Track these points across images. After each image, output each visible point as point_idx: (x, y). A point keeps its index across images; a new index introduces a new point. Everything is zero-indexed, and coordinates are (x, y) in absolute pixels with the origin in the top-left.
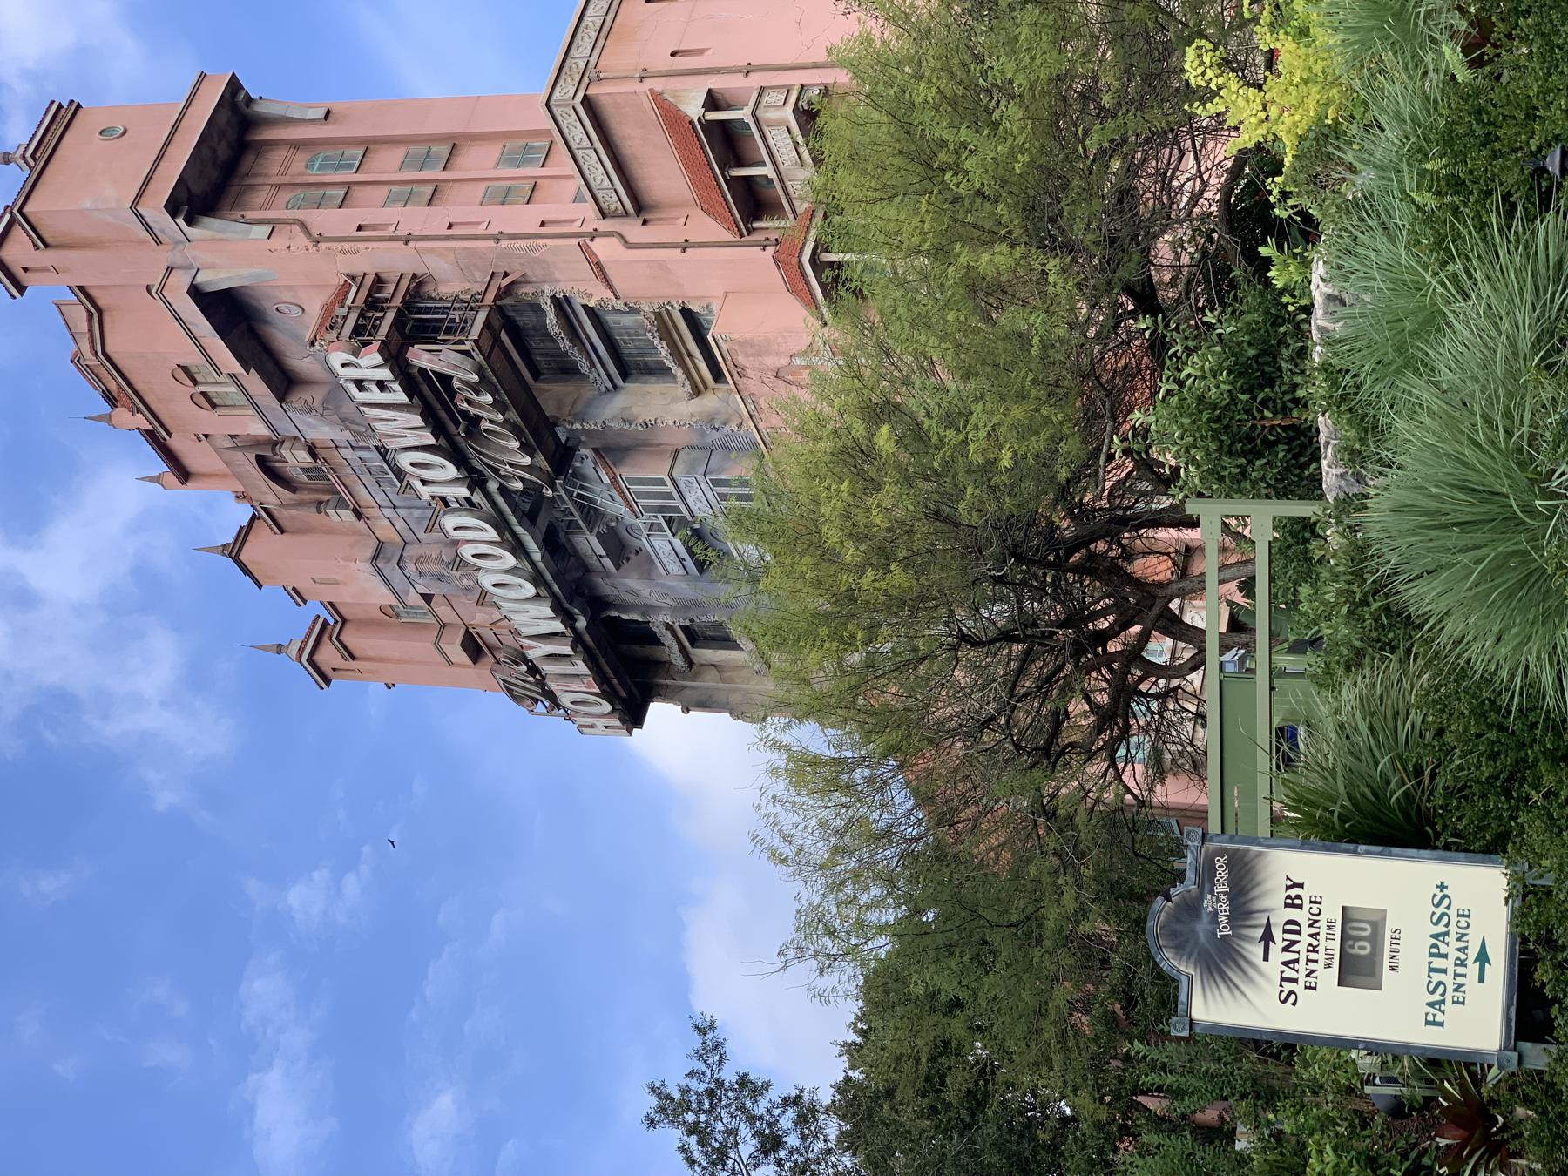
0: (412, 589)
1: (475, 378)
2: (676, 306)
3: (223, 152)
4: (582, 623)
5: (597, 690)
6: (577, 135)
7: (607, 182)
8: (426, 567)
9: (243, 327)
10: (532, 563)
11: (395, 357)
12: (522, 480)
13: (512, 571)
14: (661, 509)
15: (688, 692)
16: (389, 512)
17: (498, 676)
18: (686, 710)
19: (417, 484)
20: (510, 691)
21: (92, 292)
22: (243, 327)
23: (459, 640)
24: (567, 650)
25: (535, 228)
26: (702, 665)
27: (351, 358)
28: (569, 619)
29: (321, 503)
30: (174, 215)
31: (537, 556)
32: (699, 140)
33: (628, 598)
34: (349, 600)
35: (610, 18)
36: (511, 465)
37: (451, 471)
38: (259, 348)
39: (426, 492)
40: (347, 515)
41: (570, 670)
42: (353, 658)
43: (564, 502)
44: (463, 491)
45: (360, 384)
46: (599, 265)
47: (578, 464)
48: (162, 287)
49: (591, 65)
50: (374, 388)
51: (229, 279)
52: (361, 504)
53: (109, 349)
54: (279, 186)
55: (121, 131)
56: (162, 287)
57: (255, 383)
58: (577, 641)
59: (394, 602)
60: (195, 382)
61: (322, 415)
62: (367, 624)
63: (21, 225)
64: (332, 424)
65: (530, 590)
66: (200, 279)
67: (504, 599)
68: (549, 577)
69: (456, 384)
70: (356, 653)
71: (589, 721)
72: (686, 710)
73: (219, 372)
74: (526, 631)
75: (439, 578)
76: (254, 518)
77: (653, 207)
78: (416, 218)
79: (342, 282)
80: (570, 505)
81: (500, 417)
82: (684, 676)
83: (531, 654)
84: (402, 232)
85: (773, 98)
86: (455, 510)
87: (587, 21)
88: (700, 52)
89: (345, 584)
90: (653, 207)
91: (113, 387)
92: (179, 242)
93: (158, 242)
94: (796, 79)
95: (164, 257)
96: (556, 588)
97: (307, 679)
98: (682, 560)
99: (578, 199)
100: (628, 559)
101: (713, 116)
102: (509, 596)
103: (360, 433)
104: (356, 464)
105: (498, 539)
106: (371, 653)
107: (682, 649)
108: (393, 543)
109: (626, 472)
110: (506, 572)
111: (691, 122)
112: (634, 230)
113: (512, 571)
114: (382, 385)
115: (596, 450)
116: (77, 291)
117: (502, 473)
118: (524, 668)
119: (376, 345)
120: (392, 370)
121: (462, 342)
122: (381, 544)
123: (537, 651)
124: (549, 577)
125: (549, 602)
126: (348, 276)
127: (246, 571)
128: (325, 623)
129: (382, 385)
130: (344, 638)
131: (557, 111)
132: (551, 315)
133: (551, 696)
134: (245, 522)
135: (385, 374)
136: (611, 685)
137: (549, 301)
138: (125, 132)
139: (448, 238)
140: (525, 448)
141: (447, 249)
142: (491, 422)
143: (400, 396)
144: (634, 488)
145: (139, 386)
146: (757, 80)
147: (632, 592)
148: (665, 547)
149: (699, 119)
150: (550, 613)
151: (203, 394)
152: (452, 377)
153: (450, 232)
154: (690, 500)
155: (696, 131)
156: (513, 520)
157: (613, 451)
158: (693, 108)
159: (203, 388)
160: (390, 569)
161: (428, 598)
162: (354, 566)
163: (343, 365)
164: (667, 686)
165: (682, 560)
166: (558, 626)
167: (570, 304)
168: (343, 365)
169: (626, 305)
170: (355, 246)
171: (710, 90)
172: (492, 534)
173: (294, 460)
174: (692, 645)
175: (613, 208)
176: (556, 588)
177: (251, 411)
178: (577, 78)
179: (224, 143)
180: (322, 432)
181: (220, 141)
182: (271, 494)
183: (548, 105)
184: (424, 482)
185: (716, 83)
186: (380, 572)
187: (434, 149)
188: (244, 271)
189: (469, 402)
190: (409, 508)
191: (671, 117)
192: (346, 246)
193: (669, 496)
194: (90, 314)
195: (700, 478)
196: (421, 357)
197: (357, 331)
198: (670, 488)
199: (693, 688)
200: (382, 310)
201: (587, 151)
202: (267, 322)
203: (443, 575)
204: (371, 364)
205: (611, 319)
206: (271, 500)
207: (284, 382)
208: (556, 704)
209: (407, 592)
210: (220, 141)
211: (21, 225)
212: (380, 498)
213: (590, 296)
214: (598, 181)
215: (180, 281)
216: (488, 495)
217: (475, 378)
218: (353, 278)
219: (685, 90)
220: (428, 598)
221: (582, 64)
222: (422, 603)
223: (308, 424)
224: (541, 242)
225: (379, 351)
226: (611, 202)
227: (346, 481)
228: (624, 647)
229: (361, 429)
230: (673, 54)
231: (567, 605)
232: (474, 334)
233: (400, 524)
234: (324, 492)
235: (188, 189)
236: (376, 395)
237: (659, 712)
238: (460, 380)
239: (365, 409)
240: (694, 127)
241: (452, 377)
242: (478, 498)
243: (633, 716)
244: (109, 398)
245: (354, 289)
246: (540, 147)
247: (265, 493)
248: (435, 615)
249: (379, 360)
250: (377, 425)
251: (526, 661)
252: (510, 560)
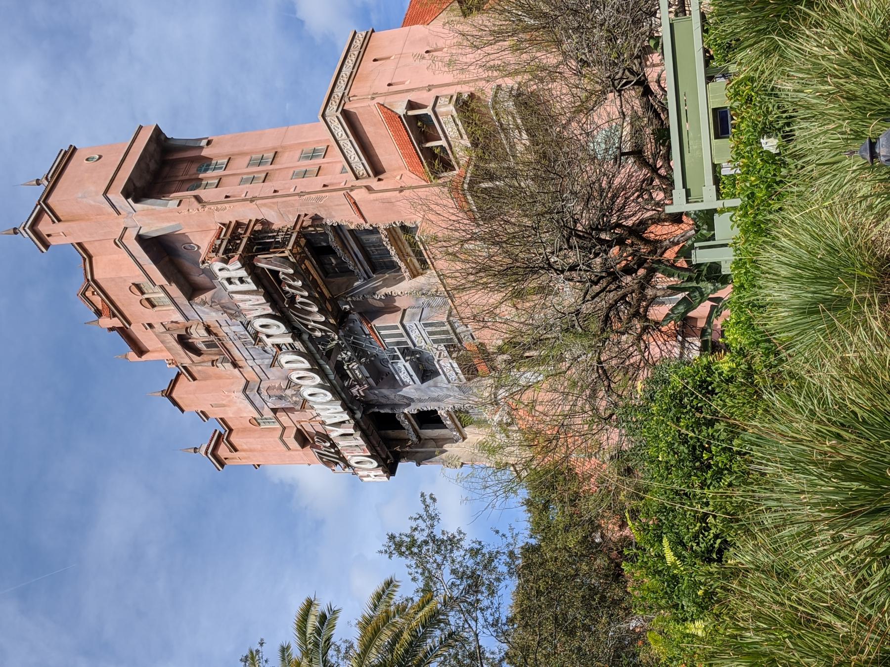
0: (265, 406)
1: (291, 271)
2: (398, 224)
3: (153, 166)
4: (358, 415)
5: (369, 454)
6: (339, 132)
7: (357, 158)
8: (271, 393)
9: (167, 259)
10: (330, 381)
11: (248, 263)
12: (321, 330)
14: (398, 343)
15: (419, 455)
16: (251, 362)
17: (314, 450)
18: (419, 464)
19: (264, 338)
20: (321, 459)
21: (87, 246)
22: (167, 259)
23: (293, 436)
24: (352, 431)
25: (320, 188)
26: (426, 439)
27: (224, 265)
28: (352, 413)
29: (213, 361)
30: (127, 197)
31: (332, 377)
32: (406, 129)
33: (383, 401)
34: (231, 416)
35: (355, 70)
36: (315, 322)
37: (283, 328)
38: (176, 271)
39: (269, 341)
40: (228, 366)
41: (354, 443)
42: (236, 450)
45: (229, 280)
46: (355, 203)
47: (352, 325)
48: (121, 238)
49: (346, 94)
50: (238, 282)
51: (157, 230)
52: (236, 359)
53: (96, 277)
54: (183, 181)
55: (98, 157)
56: (121, 238)
57: (174, 290)
58: (357, 426)
59: (257, 416)
60: (143, 293)
61: (211, 306)
62: (244, 430)
63: (47, 214)
64: (218, 310)
65: (330, 396)
66: (141, 232)
67: (315, 402)
68: (339, 389)
69: (282, 276)
70: (238, 448)
71: (366, 473)
72: (419, 464)
73: (154, 284)
74: (328, 422)
75: (280, 398)
76: (178, 375)
77: (383, 172)
78: (257, 189)
79: (218, 228)
81: (306, 294)
82: (416, 446)
83: (333, 435)
84: (249, 196)
85: (441, 101)
86: (285, 353)
87: (342, 74)
88: (403, 83)
89: (229, 406)
90: (383, 172)
91: (100, 307)
92: (130, 213)
93: (119, 213)
94: (453, 91)
95: (123, 222)
96: (343, 395)
97: (210, 464)
98: (411, 376)
99: (343, 171)
100: (382, 379)
101: (411, 113)
102: (318, 401)
103: (232, 315)
104: (231, 335)
105: (310, 367)
106: (245, 447)
107: (415, 431)
108: (255, 381)
109: (377, 323)
110: (315, 386)
111: (400, 117)
112: (373, 183)
114: (241, 280)
115: (360, 314)
116: (76, 246)
117: (309, 327)
118: (328, 444)
119: (237, 257)
120: (246, 270)
121: (283, 252)
122: (248, 382)
123: (335, 433)
124: (339, 389)
125: (340, 402)
126: (221, 224)
127: (175, 403)
128: (220, 433)
129: (241, 280)
130: (232, 439)
131: (328, 119)
132: (331, 236)
133: (343, 459)
134: (174, 378)
135: (243, 273)
136: (377, 451)
137: (329, 229)
138: (100, 157)
139: (273, 197)
140: (320, 311)
141: (274, 203)
142: (302, 296)
143: (253, 287)
144: (383, 332)
145: (113, 297)
146: (434, 93)
147: (385, 397)
148: (403, 369)
149: (404, 115)
150: (341, 409)
151: (148, 300)
152: (279, 272)
153: (275, 194)
154: (413, 336)
155: (402, 122)
157: (371, 313)
158: (401, 110)
159: (146, 296)
160: (253, 394)
161: (275, 411)
162: (233, 395)
164: (408, 452)
165: (411, 376)
166: (346, 417)
167: (341, 230)
168: (220, 270)
169: (371, 225)
170: (224, 206)
171: (409, 101)
172: (307, 365)
173: (198, 336)
174: (420, 429)
175: (361, 174)
176: (343, 395)
177: (173, 307)
178: (338, 101)
179: (153, 161)
180: (212, 316)
181: (150, 160)
182: (185, 358)
183: (323, 116)
184: (268, 336)
185: (414, 97)
186: (247, 397)
187: (265, 155)
188: (165, 225)
189: (290, 286)
190: (262, 359)
191: (387, 111)
192: (219, 206)
193: (401, 335)
194: (85, 260)
195: (417, 323)
196: (263, 262)
197: (226, 251)
198: (401, 331)
199: (422, 452)
200: (240, 239)
201: (346, 141)
202: (179, 256)
203: (282, 396)
204: (235, 269)
205: (364, 238)
206: (187, 362)
207: (192, 290)
208: (348, 465)
209: (263, 408)
210: (150, 160)
211: (47, 214)
212: (246, 354)
213: (352, 223)
214: (352, 158)
215: (131, 234)
216: (303, 342)
217: (291, 271)
218: (224, 225)
219: (396, 102)
220: (275, 411)
221: (340, 95)
222: (272, 414)
223: (203, 312)
224: (324, 195)
225: (239, 260)
226: (360, 170)
227: (228, 347)
228: (383, 432)
229: (233, 312)
230: (389, 85)
231: (350, 405)
232: (290, 247)
233: (258, 369)
234: (216, 354)
235: (134, 185)
237: (404, 467)
238: (283, 273)
239: (233, 295)
240: (401, 120)
241: (279, 272)
242: (298, 345)
243: (390, 470)
244: (99, 313)
245: (225, 230)
246: (322, 149)
247: (183, 358)
248: (279, 422)
249: (239, 265)
250: (240, 304)
251: (330, 440)
252: (318, 380)
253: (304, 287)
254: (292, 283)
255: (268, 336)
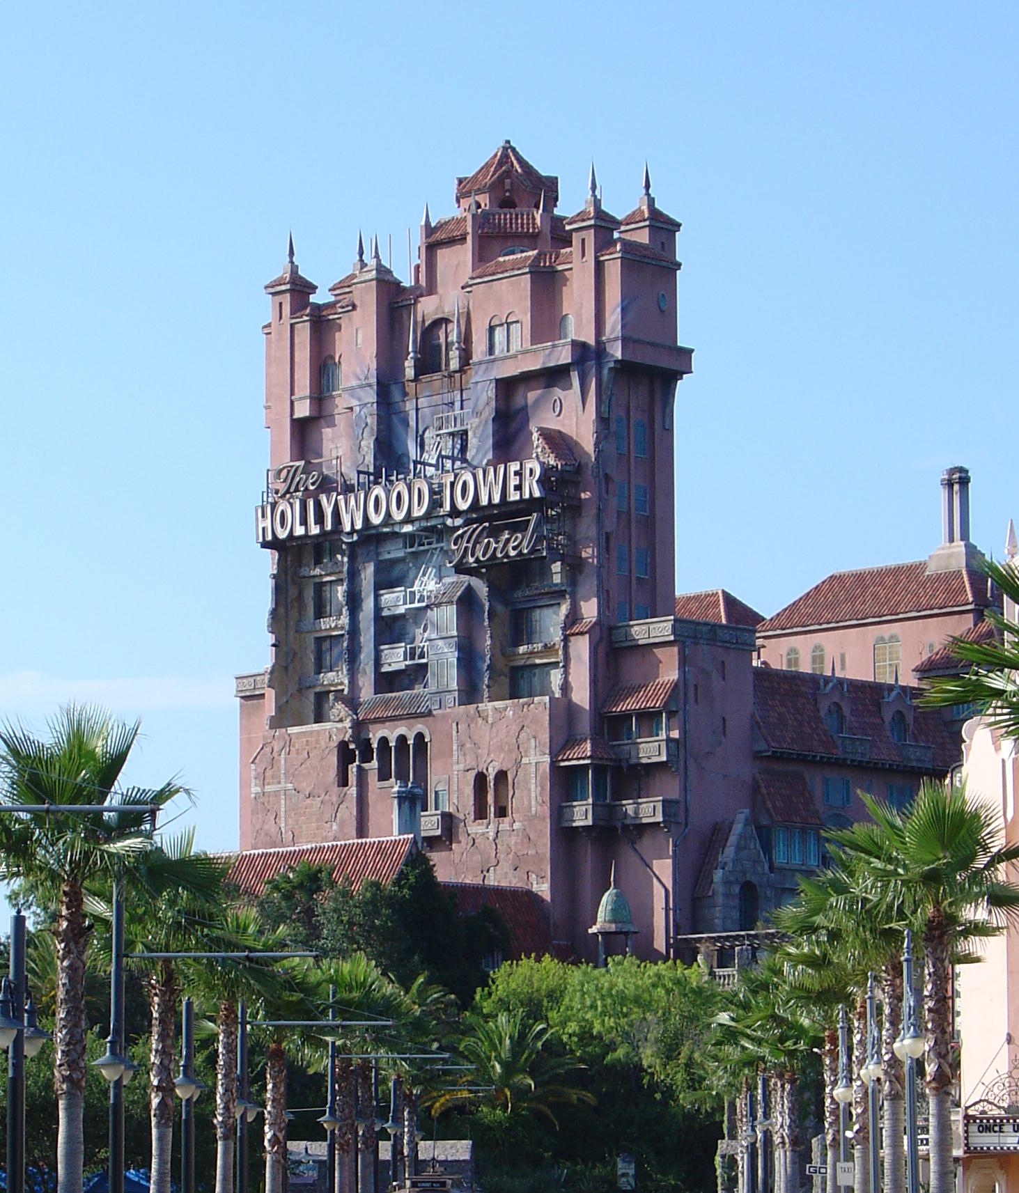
13: (388, 515)
36: (466, 548)
43: (429, 544)
44: (447, 507)
45: (516, 473)
50: (517, 483)
69: (519, 535)
80: (426, 547)
88: (696, 701)
113: (388, 515)
114: (519, 488)
129: (519, 488)
138: (662, 311)
142: (495, 549)
143: (514, 496)
148: (395, 601)
156: (424, 524)
163: (531, 470)
166: (348, 528)
172: (418, 512)
177: (488, 358)
184: (452, 484)
189: (508, 541)
209: (352, 396)
230: (696, 686)
236: (513, 481)
249: (537, 494)
252: (398, 516)
253: (507, 556)
254: (512, 544)
255: (452, 484)
